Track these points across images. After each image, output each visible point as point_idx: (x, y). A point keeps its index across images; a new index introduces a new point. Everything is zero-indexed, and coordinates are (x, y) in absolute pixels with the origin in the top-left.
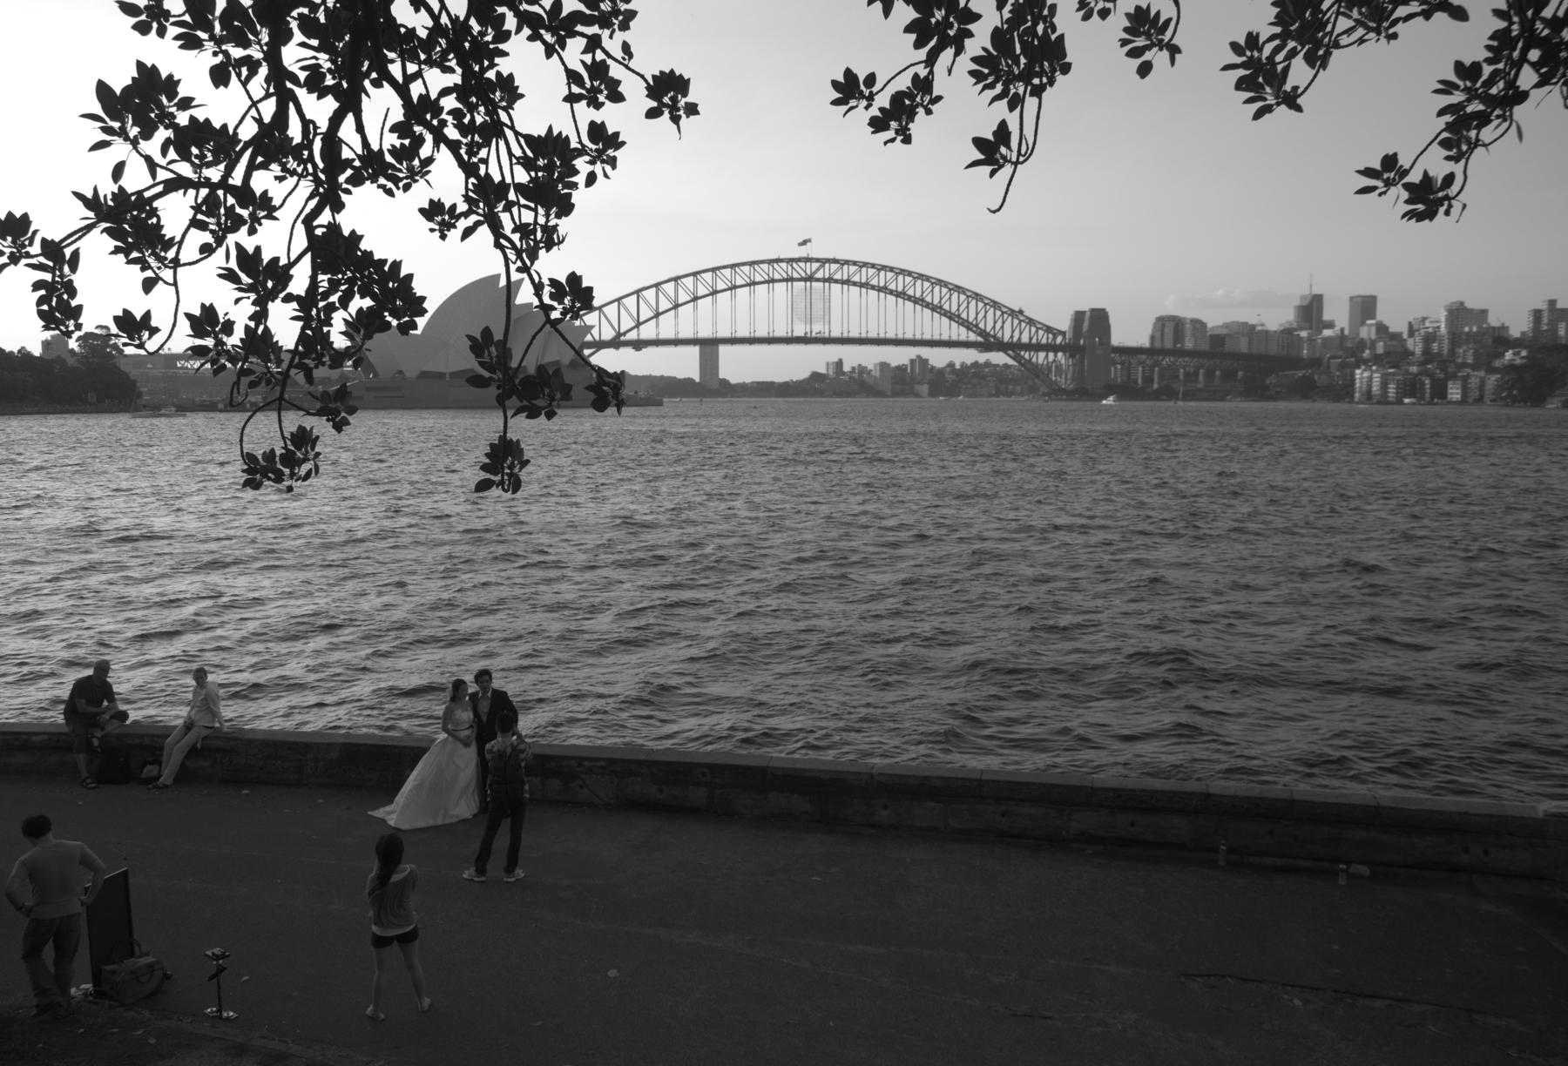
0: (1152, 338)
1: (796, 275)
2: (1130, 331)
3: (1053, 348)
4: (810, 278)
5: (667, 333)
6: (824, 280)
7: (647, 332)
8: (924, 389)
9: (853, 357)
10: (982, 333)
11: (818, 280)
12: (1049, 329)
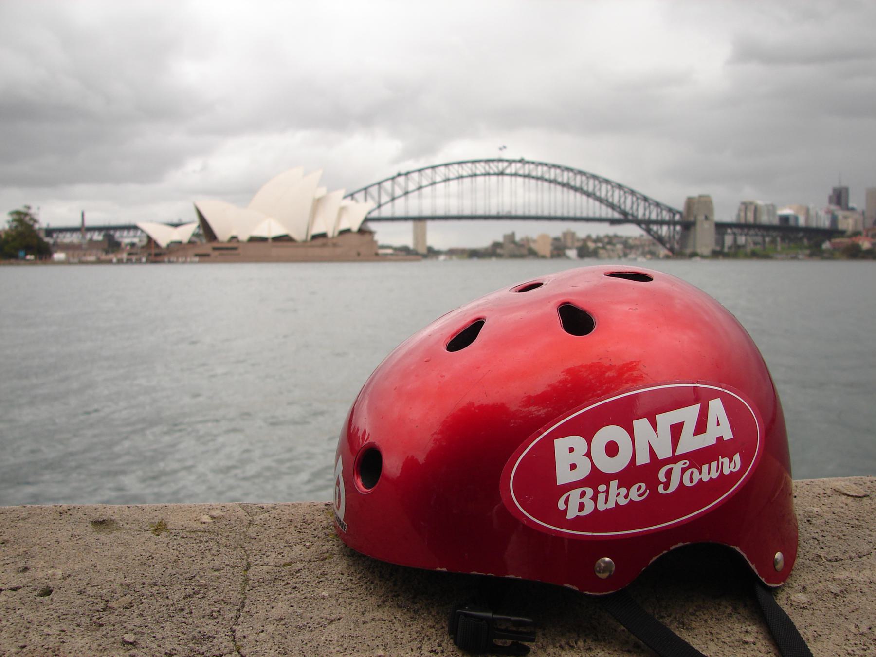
0: (739, 215)
1: (491, 172)
2: (725, 214)
3: (675, 223)
4: (502, 174)
5: (399, 213)
6: (511, 175)
7: (386, 211)
8: (572, 253)
9: (523, 231)
10: (625, 213)
11: (507, 175)
12: (670, 210)
